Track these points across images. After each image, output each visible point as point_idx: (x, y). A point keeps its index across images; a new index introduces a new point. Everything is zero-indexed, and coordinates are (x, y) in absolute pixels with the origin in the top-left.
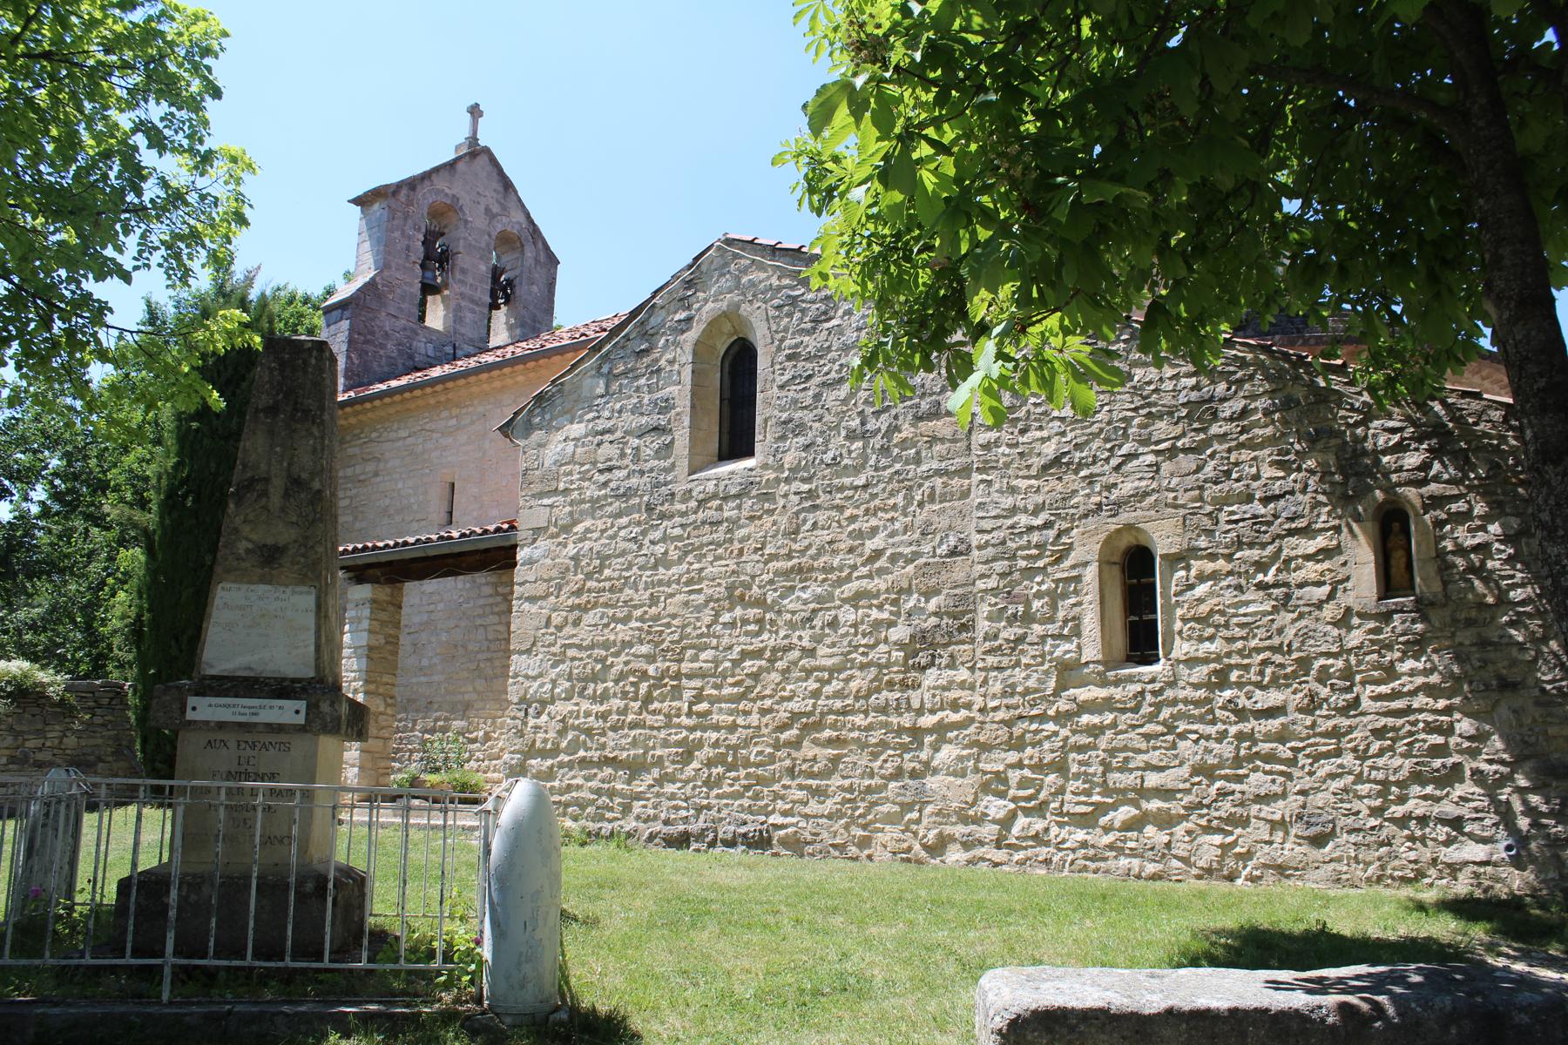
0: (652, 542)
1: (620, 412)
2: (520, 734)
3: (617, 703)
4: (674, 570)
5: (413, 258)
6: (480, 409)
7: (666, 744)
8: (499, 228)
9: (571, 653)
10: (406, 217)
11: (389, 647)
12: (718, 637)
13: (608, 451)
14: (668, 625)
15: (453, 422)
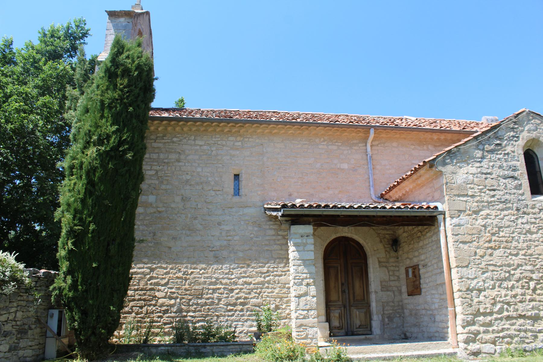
0: (522, 223)
1: (493, 167)
3: (519, 291)
4: (534, 236)
9: (491, 268)
14: (538, 258)
15: (240, 144)
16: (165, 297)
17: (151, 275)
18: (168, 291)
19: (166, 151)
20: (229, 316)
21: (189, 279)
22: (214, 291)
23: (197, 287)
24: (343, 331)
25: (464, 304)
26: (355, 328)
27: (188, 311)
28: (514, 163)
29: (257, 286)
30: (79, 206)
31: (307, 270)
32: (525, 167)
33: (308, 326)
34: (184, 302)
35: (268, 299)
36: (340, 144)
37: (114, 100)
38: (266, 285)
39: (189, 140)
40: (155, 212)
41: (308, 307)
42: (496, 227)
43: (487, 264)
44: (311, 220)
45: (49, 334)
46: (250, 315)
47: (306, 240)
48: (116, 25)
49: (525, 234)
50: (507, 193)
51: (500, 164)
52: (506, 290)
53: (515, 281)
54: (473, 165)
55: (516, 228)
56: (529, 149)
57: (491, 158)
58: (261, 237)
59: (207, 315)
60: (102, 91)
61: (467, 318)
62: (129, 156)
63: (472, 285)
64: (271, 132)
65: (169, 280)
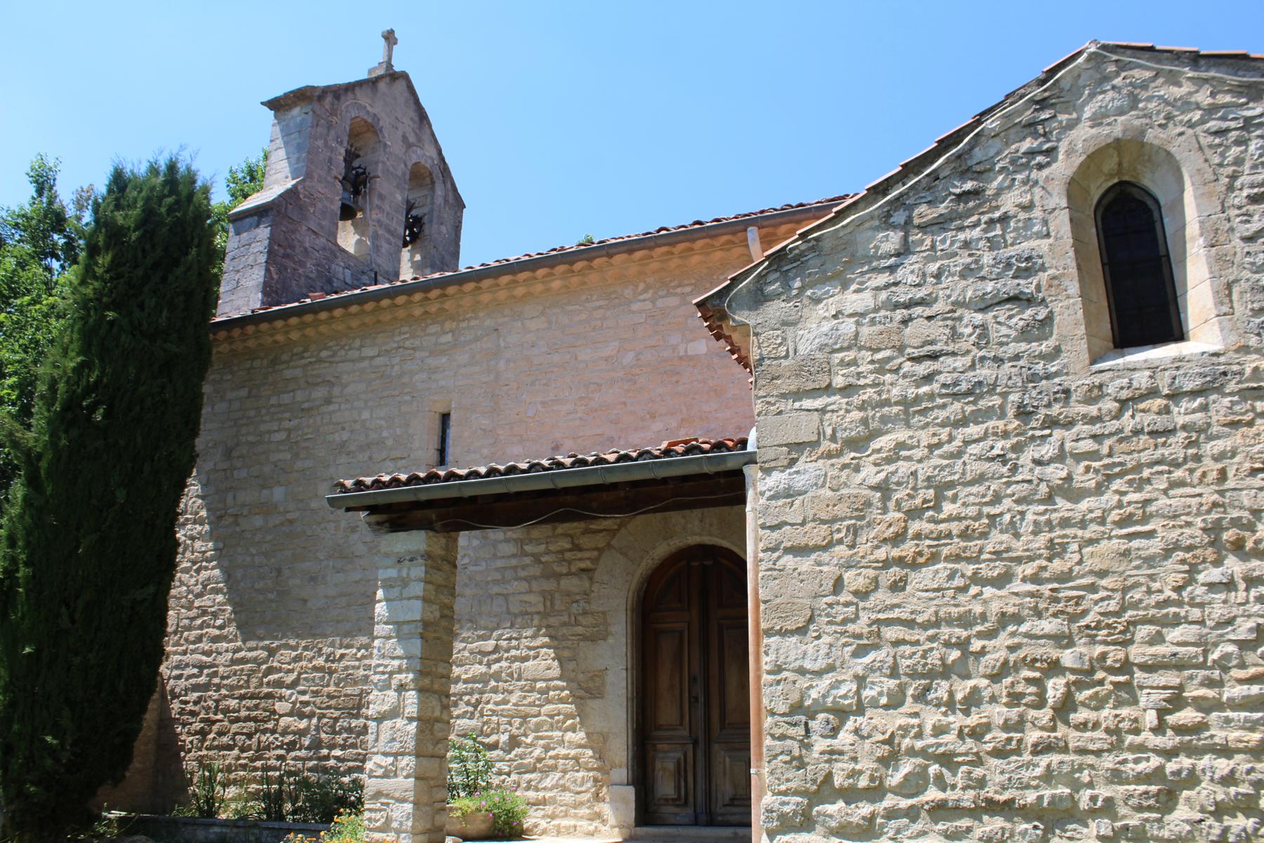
0: (1038, 462)
1: (938, 276)
2: (801, 764)
3: (998, 713)
5: (335, 173)
6: (488, 322)
7: (1116, 777)
8: (414, 159)
9: (891, 633)
10: (330, 126)
11: (444, 623)
12: (1201, 605)
13: (917, 332)
14: (1092, 588)
15: (449, 337)
16: (290, 714)
17: (270, 664)
18: (297, 699)
19: (308, 383)
21: (336, 671)
23: (349, 690)
24: (690, 811)
25: (775, 757)
26: (720, 803)
27: (332, 747)
28: (1025, 246)
29: (470, 685)
31: (403, 648)
32: (1071, 254)
33: (392, 798)
34: (325, 725)
35: (495, 718)
36: (688, 289)
38: (493, 683)
39: (350, 349)
40: (282, 524)
41: (396, 746)
42: (928, 488)
43: (878, 621)
44: (434, 517)
47: (409, 569)
49: (1049, 499)
50: (983, 359)
51: (969, 260)
52: (943, 709)
53: (985, 676)
54: (862, 283)
55: (1008, 484)
56: (1121, 183)
57: (933, 247)
58: (484, 564)
61: (783, 803)
63: (814, 694)
65: (300, 674)
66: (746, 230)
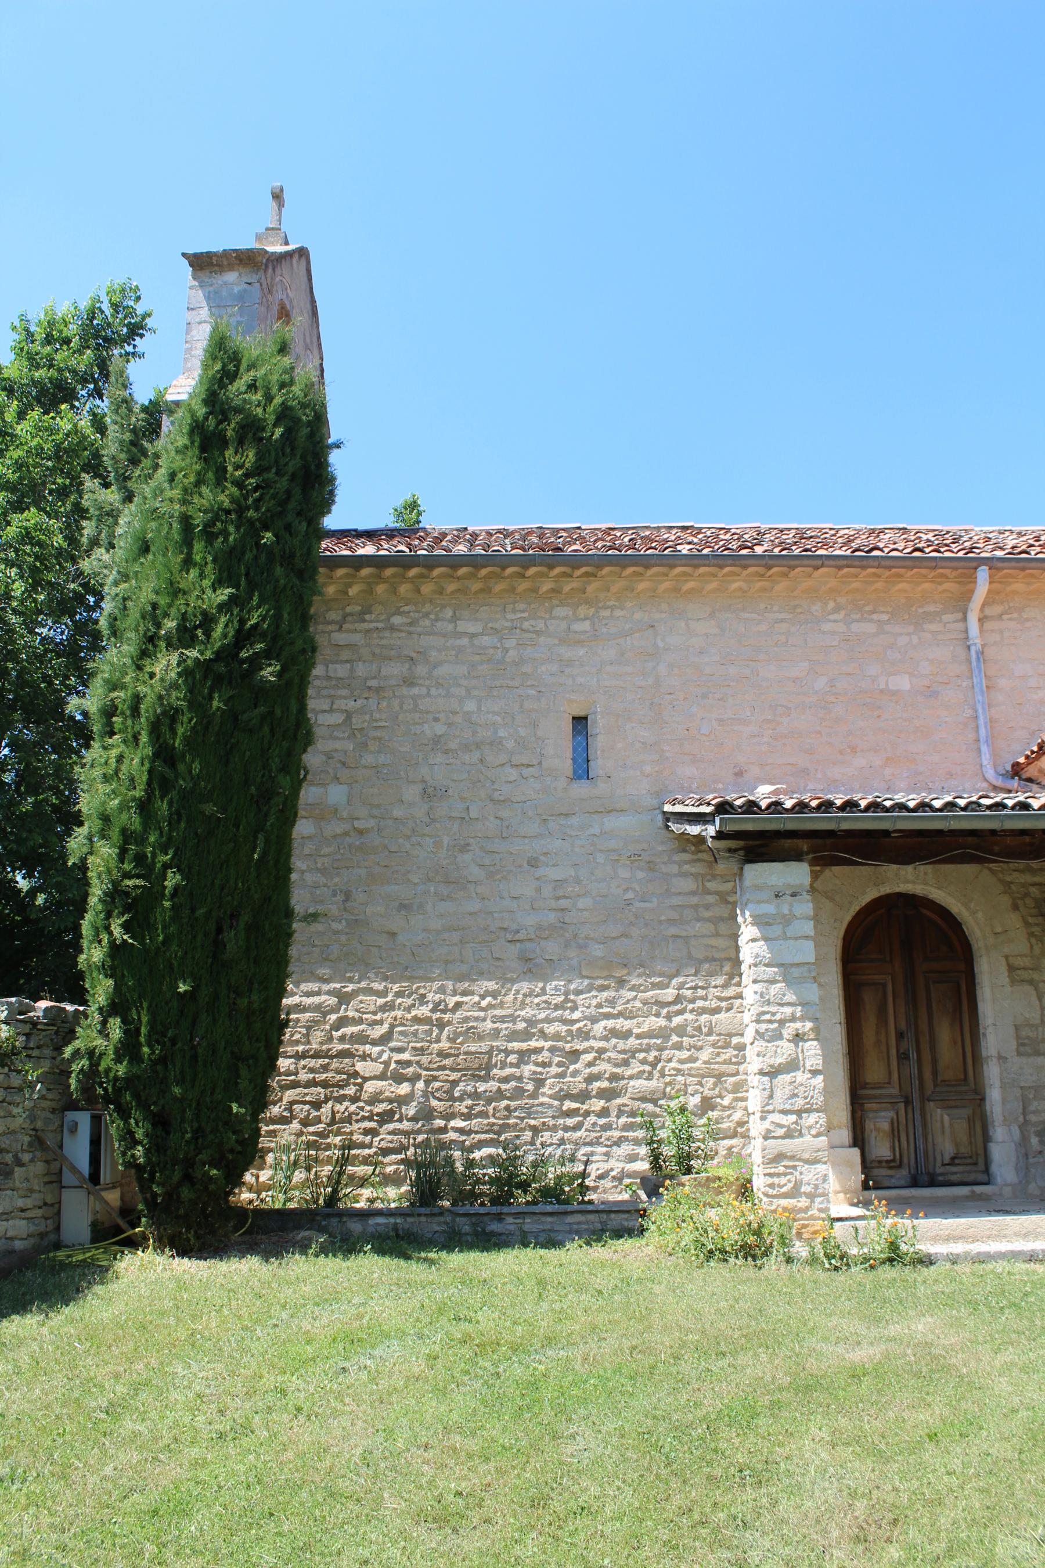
15: (586, 626)
16: (382, 1077)
17: (342, 1013)
18: (390, 1058)
19: (374, 654)
20: (566, 1129)
21: (449, 1023)
22: (524, 1056)
24: (904, 1172)
26: (939, 1163)
27: (449, 1117)
29: (646, 1041)
30: (134, 822)
31: (795, 994)
33: (800, 1160)
34: (438, 1090)
35: (679, 1078)
36: (885, 617)
37: (218, 514)
38: (675, 1038)
39: (436, 620)
40: (346, 834)
41: (799, 1103)
44: (805, 848)
45: (68, 1178)
46: (628, 1127)
47: (791, 905)
48: (216, 293)
58: (655, 900)
59: (505, 1128)
60: (185, 490)
62: (269, 672)
64: (676, 590)
65: (392, 1027)
66: (976, 568)
